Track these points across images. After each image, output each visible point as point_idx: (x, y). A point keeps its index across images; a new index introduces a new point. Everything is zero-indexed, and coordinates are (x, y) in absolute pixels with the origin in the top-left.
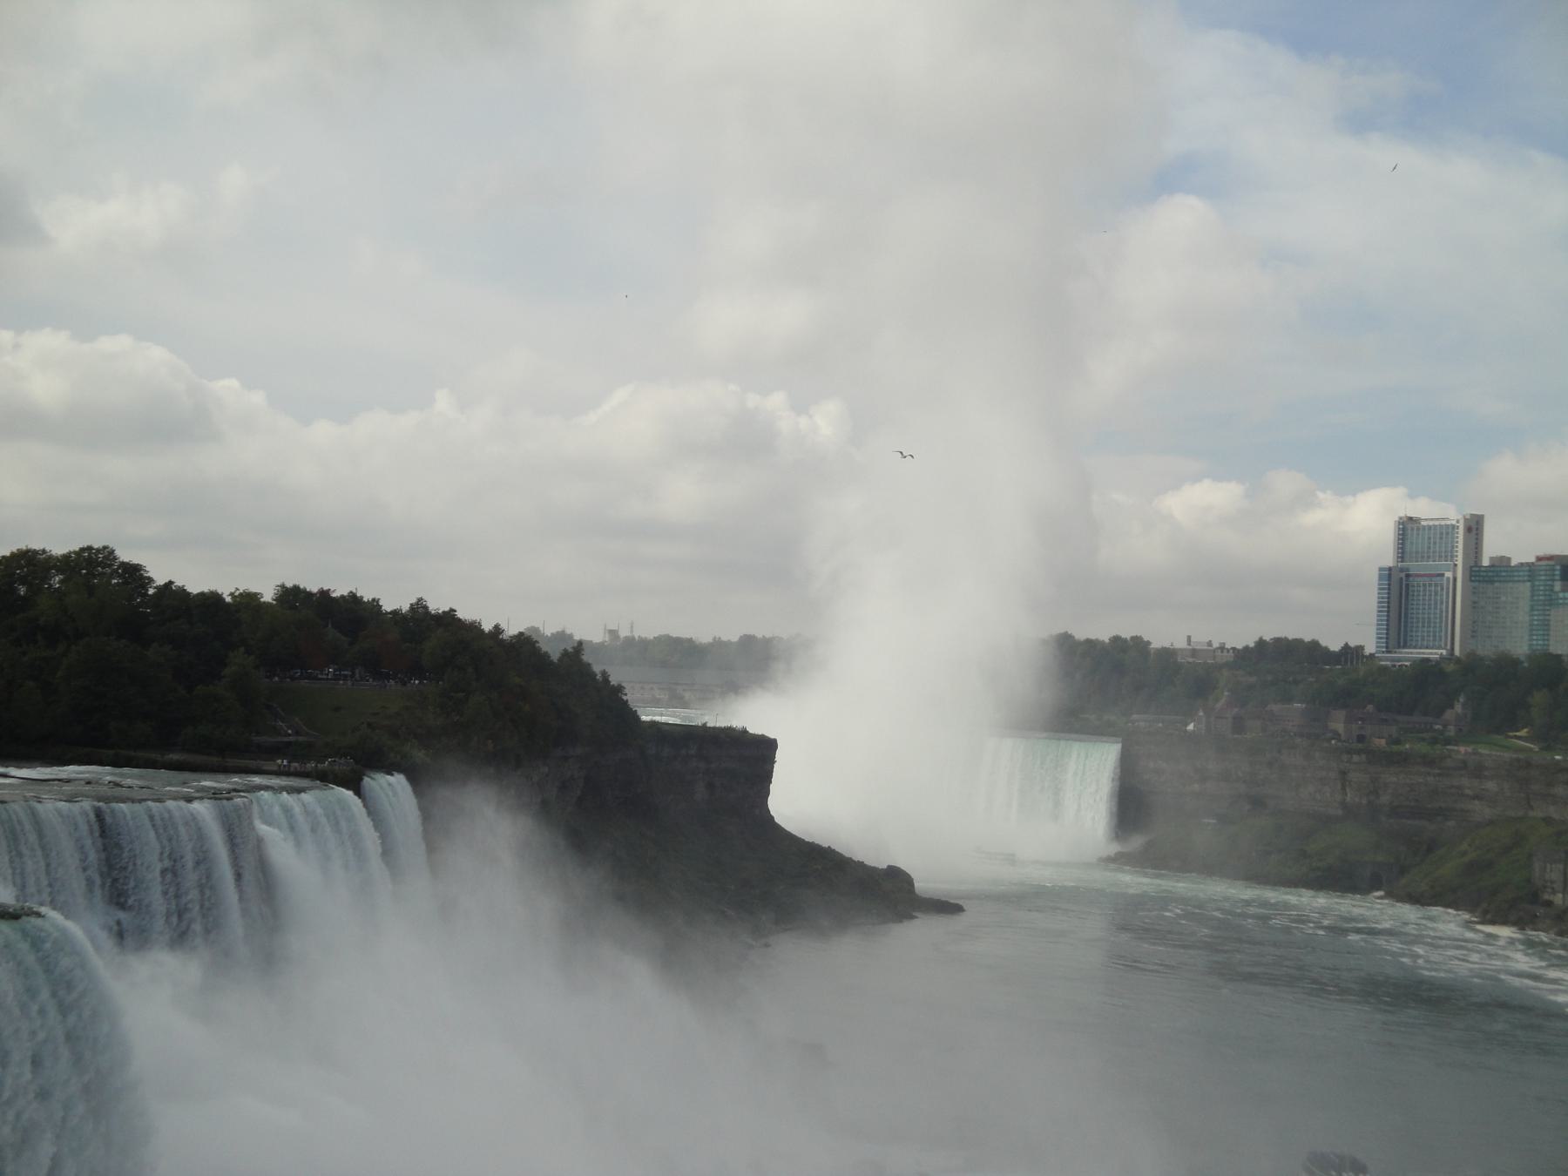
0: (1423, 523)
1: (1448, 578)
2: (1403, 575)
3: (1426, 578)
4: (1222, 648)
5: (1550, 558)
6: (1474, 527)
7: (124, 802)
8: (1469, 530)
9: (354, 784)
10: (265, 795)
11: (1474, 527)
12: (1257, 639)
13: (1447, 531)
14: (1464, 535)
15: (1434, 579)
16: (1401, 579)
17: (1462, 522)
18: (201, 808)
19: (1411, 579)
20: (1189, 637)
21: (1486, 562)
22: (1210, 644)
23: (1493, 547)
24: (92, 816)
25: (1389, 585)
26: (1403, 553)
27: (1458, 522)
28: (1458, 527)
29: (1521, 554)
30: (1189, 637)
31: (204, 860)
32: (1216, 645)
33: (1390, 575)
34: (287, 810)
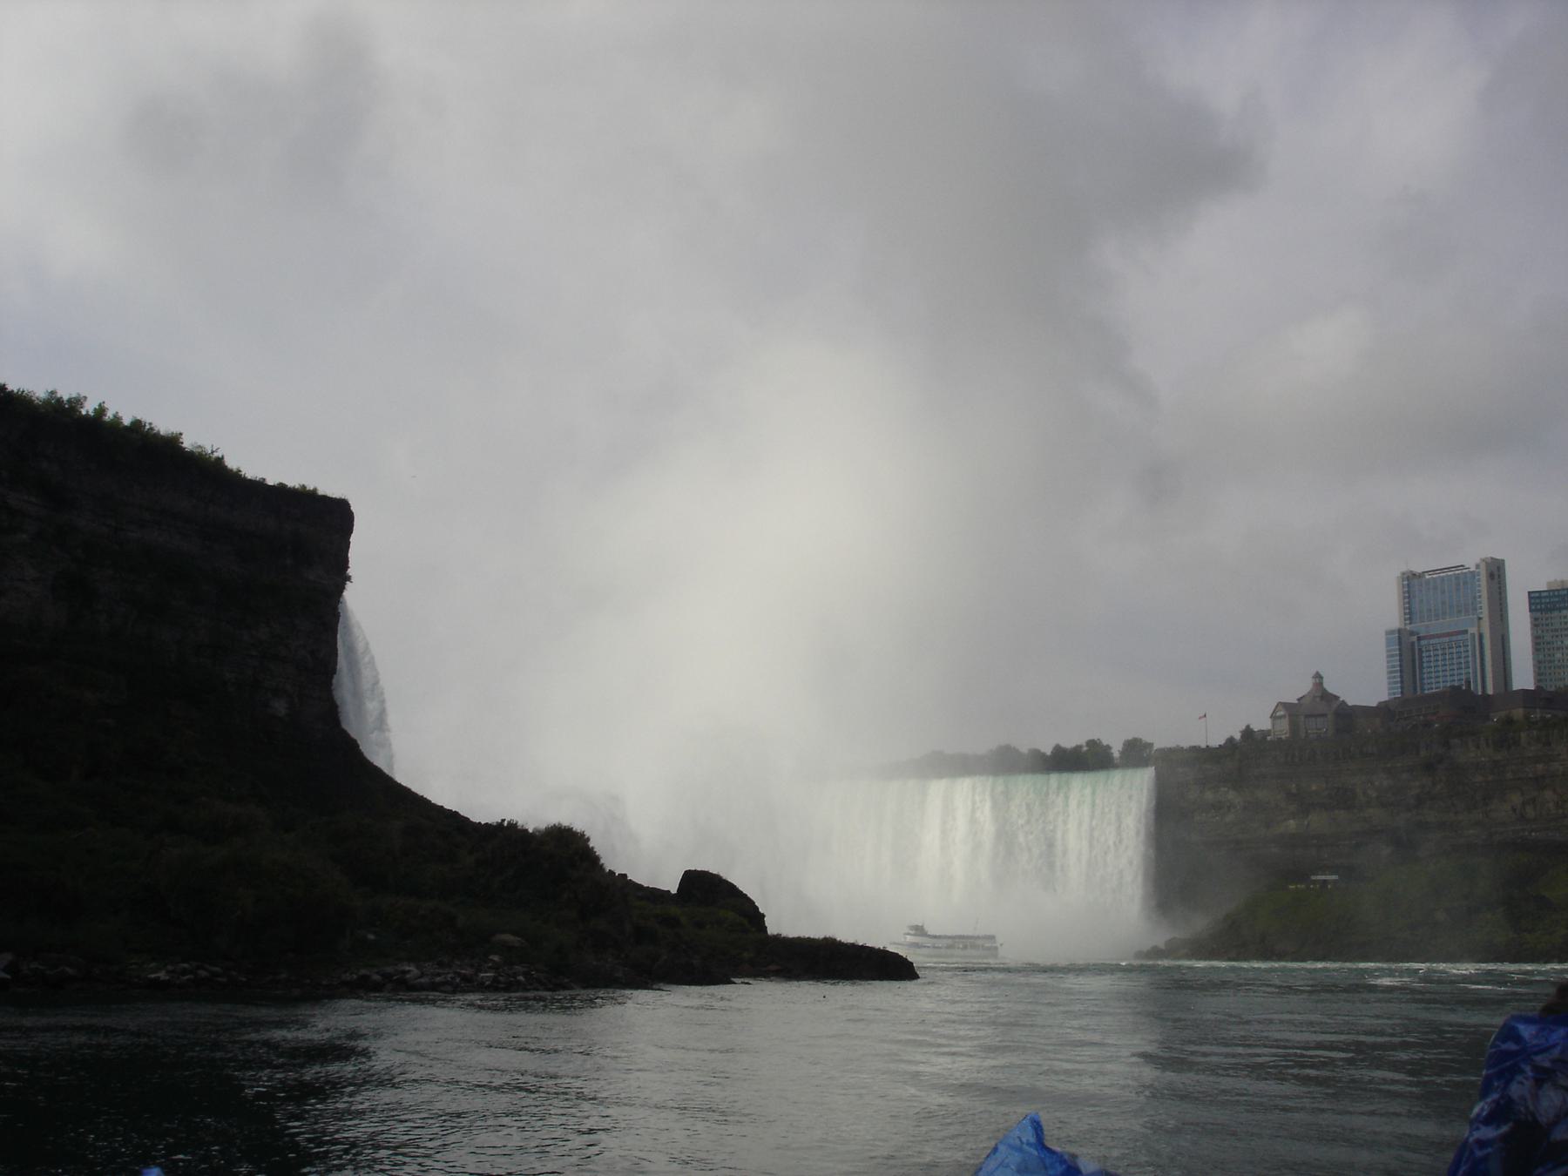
1: (1473, 635)
2: (1414, 638)
3: (1447, 639)
8: (1491, 576)
11: (1496, 573)
13: (1459, 579)
14: (1487, 582)
15: (1454, 638)
16: (1413, 644)
17: (1483, 566)
19: (1423, 642)
25: (1400, 650)
26: (1410, 613)
27: (1478, 566)
28: (1479, 574)
33: (1400, 638)
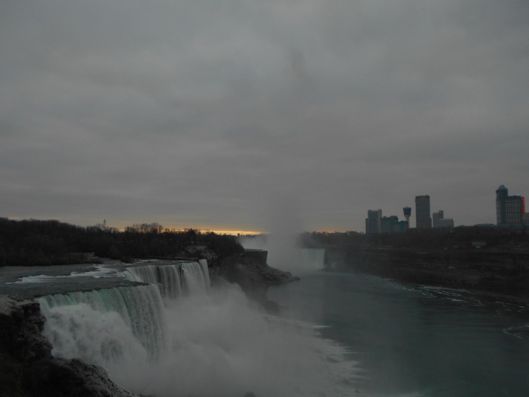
4: (341, 232)
5: (393, 216)
6: (380, 211)
7: (161, 265)
9: (197, 261)
10: (183, 263)
12: (346, 231)
18: (173, 266)
21: (383, 217)
23: (384, 215)
24: (157, 268)
29: (388, 215)
30: (335, 231)
31: (174, 275)
32: (340, 232)
34: (187, 265)
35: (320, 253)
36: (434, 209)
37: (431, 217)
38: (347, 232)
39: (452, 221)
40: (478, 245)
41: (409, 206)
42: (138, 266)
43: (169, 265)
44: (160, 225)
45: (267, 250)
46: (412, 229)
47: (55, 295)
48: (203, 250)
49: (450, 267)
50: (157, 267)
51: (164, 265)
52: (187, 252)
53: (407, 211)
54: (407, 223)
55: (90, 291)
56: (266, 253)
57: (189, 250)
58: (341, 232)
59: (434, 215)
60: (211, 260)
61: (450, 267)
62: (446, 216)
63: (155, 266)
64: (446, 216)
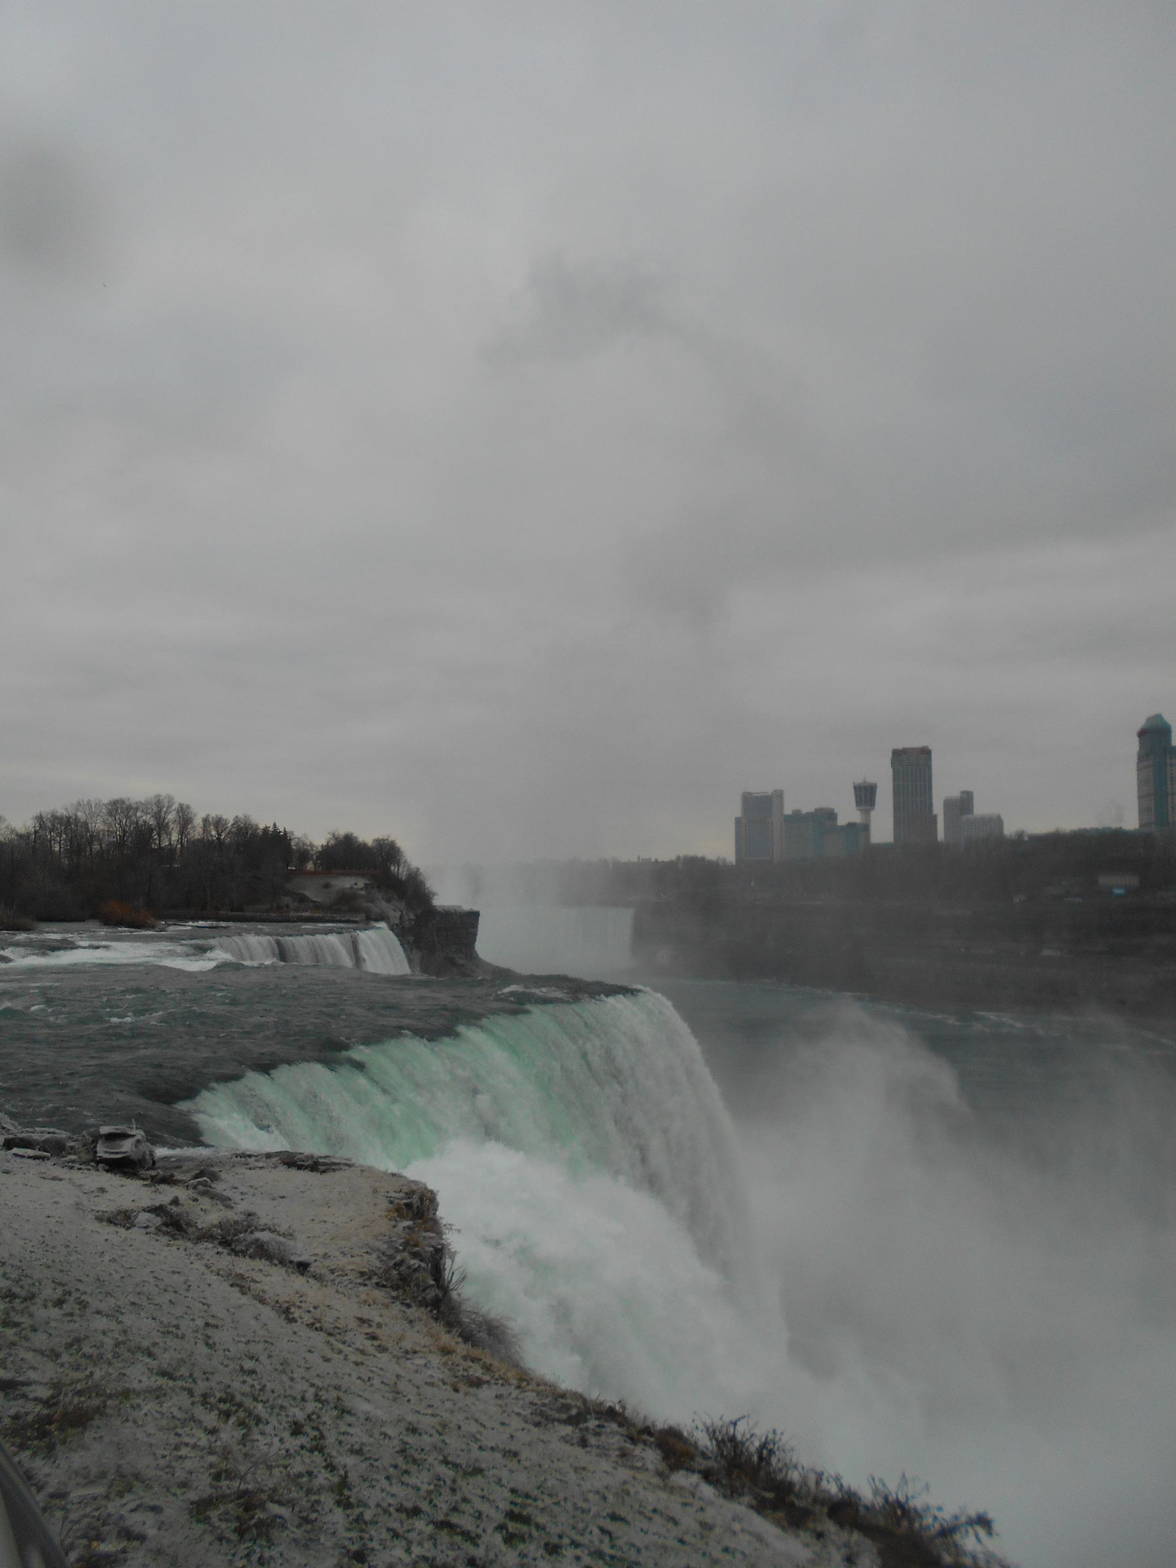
0: (754, 795)
4: (656, 860)
5: (821, 809)
6: (779, 795)
7: (290, 935)
18: (333, 939)
20: (639, 858)
21: (788, 811)
22: (650, 859)
24: (275, 946)
29: (807, 807)
30: (639, 858)
32: (653, 860)
35: (621, 921)
36: (943, 789)
37: (938, 809)
38: (678, 858)
39: (998, 821)
40: (1118, 884)
41: (871, 780)
42: (214, 938)
43: (318, 937)
44: (181, 806)
45: (475, 909)
46: (883, 848)
47: (283, 1074)
48: (363, 893)
49: (1046, 952)
50: (278, 943)
51: (301, 935)
52: (302, 899)
53: (865, 795)
54: (866, 828)
55: (449, 1032)
56: (474, 916)
57: (307, 893)
58: (656, 860)
59: (948, 804)
60: (397, 925)
61: (1046, 952)
62: (981, 808)
63: (269, 938)
64: (981, 808)
